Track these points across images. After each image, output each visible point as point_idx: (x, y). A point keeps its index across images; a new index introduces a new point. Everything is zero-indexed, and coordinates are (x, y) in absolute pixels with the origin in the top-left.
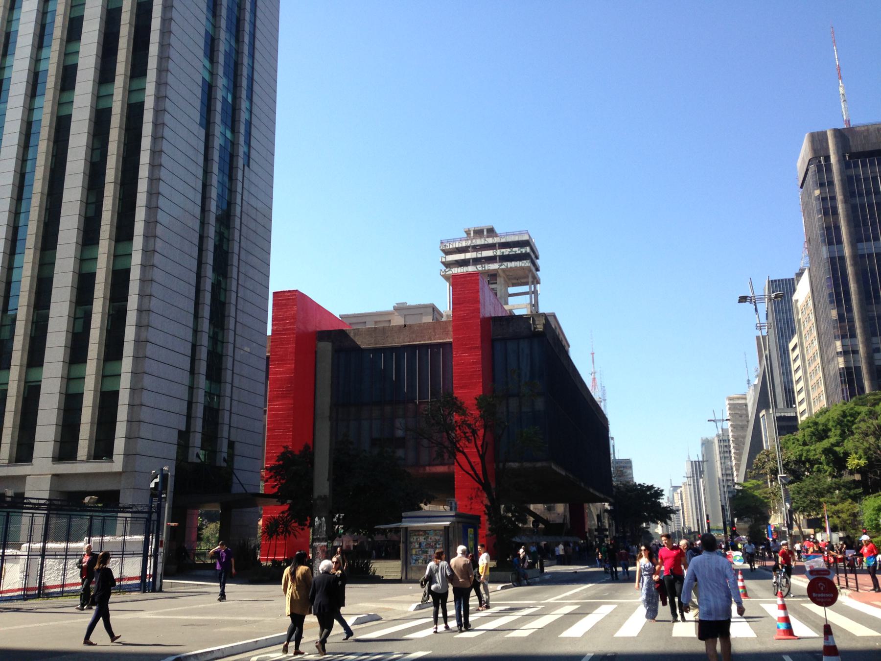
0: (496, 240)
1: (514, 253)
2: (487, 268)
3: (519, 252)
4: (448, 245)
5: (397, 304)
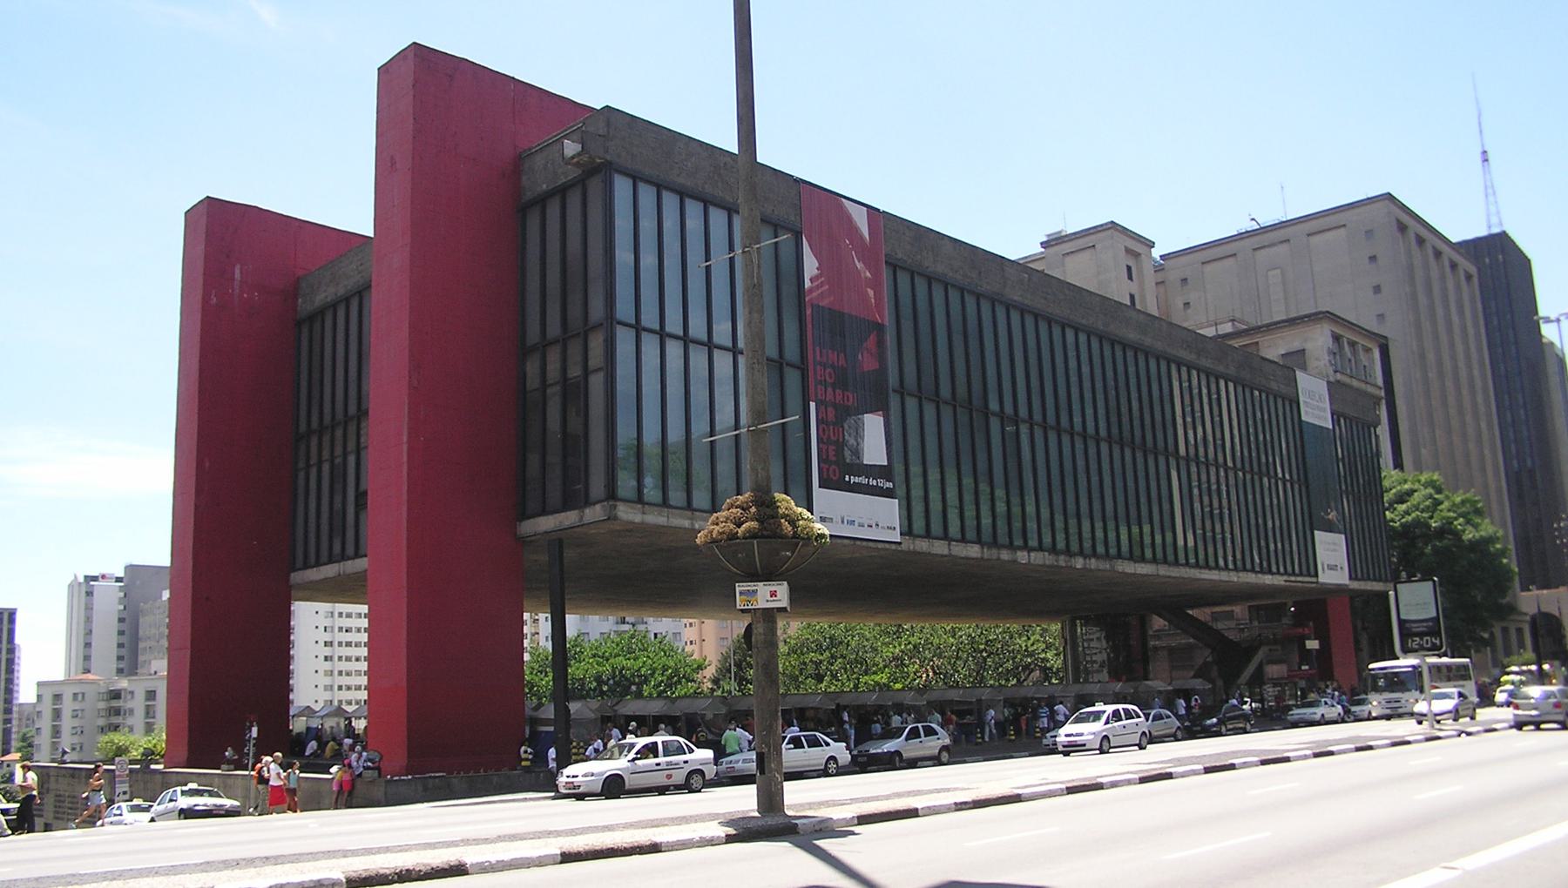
5: (1048, 236)
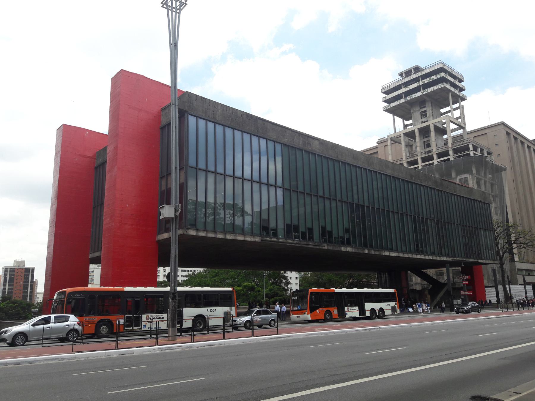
0: (420, 74)
1: (432, 80)
2: (413, 97)
3: (436, 78)
4: (387, 88)
